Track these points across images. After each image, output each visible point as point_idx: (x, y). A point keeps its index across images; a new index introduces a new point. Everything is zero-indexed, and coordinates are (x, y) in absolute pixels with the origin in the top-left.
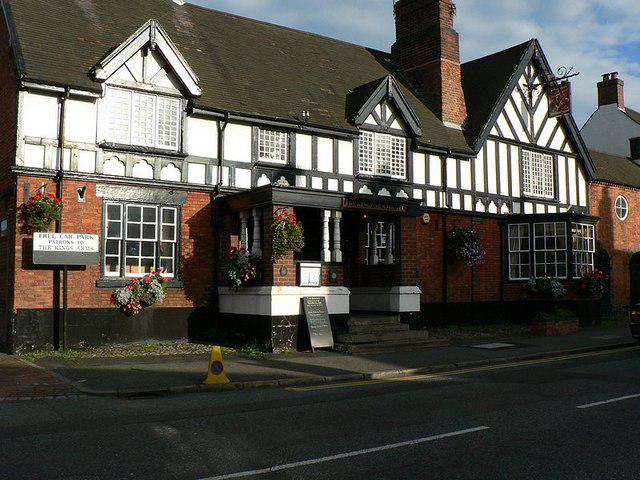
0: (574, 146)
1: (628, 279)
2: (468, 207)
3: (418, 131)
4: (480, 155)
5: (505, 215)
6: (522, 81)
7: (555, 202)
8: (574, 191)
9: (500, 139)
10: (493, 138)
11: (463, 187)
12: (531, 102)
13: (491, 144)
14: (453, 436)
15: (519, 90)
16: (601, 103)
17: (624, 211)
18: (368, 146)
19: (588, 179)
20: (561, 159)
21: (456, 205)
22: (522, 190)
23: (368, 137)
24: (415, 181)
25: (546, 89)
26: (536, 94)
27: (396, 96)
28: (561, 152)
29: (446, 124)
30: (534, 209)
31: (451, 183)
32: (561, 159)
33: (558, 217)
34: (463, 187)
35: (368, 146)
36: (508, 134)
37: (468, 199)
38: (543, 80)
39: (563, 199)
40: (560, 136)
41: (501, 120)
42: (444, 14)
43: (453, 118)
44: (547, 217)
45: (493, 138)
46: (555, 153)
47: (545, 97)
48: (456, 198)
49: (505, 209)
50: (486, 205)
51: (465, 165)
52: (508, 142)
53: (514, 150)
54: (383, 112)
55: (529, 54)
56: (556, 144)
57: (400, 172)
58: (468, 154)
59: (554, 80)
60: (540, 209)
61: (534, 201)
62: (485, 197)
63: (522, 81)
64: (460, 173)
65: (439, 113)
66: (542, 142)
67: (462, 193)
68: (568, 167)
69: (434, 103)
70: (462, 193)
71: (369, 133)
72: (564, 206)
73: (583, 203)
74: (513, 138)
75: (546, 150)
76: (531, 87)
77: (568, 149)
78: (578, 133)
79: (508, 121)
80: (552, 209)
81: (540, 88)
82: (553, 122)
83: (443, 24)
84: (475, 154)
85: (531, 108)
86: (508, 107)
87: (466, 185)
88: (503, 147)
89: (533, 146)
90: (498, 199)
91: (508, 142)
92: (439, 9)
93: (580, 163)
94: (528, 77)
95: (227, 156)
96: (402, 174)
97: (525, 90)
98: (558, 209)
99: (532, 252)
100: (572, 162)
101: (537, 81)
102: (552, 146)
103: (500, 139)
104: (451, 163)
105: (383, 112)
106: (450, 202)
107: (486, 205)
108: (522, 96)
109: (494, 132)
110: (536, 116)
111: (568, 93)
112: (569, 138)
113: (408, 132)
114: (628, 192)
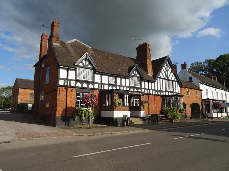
0: (177, 79)
1: (190, 109)
2: (154, 93)
3: (96, 68)
4: (156, 82)
5: (162, 95)
6: (165, 65)
7: (173, 92)
8: (177, 89)
9: (160, 78)
10: (159, 78)
11: (127, 85)
12: (167, 69)
13: (158, 79)
14: (138, 145)
15: (165, 67)
16: (182, 69)
17: (189, 94)
18: (86, 73)
19: (180, 87)
20: (174, 82)
21: (151, 93)
22: (165, 89)
23: (86, 70)
24: (118, 84)
25: (171, 67)
26: (168, 68)
27: (90, 59)
28: (174, 81)
29: (148, 75)
30: (168, 94)
31: (150, 88)
32: (174, 82)
33: (174, 95)
34: (127, 85)
35: (84, 72)
36: (162, 77)
37: (154, 91)
38: (170, 64)
39: (175, 91)
40: (174, 77)
41: (161, 74)
42: (148, 50)
43: (150, 74)
44: (171, 95)
45: (159, 78)
46: (173, 81)
47: (170, 69)
48: (151, 91)
49: (162, 94)
50: (158, 93)
51: (153, 84)
52: (162, 79)
53: (164, 80)
54: (86, 63)
55: (167, 59)
56: (173, 79)
57: (91, 79)
58: (154, 82)
59: (172, 65)
60: (170, 94)
61: (168, 92)
62: (158, 91)
63: (165, 65)
64: (152, 86)
65: (147, 72)
66: (170, 79)
67: (152, 90)
68: (176, 84)
69: (146, 70)
70: (152, 90)
71: (81, 68)
72: (175, 93)
73: (179, 92)
74: (163, 78)
75: (171, 80)
76: (167, 66)
77: (175, 80)
78: (177, 75)
79: (162, 74)
80: (172, 94)
81: (169, 67)
82: (172, 74)
83: (148, 53)
84: (155, 81)
85: (167, 71)
86: (162, 71)
87: (153, 88)
88: (161, 80)
89: (168, 80)
90: (160, 91)
91: (162, 79)
92: (147, 49)
93: (178, 83)
94: (167, 64)
95: (69, 78)
96: (114, 83)
97: (166, 67)
98: (174, 94)
99: (168, 103)
100: (177, 83)
101: (168, 65)
102: (172, 79)
103: (160, 78)
104: (150, 84)
105: (86, 63)
106: (150, 92)
107: (158, 93)
108: (165, 68)
109: (159, 76)
110: (168, 73)
111: (176, 68)
112: (176, 77)
113: (93, 69)
114: (190, 89)
